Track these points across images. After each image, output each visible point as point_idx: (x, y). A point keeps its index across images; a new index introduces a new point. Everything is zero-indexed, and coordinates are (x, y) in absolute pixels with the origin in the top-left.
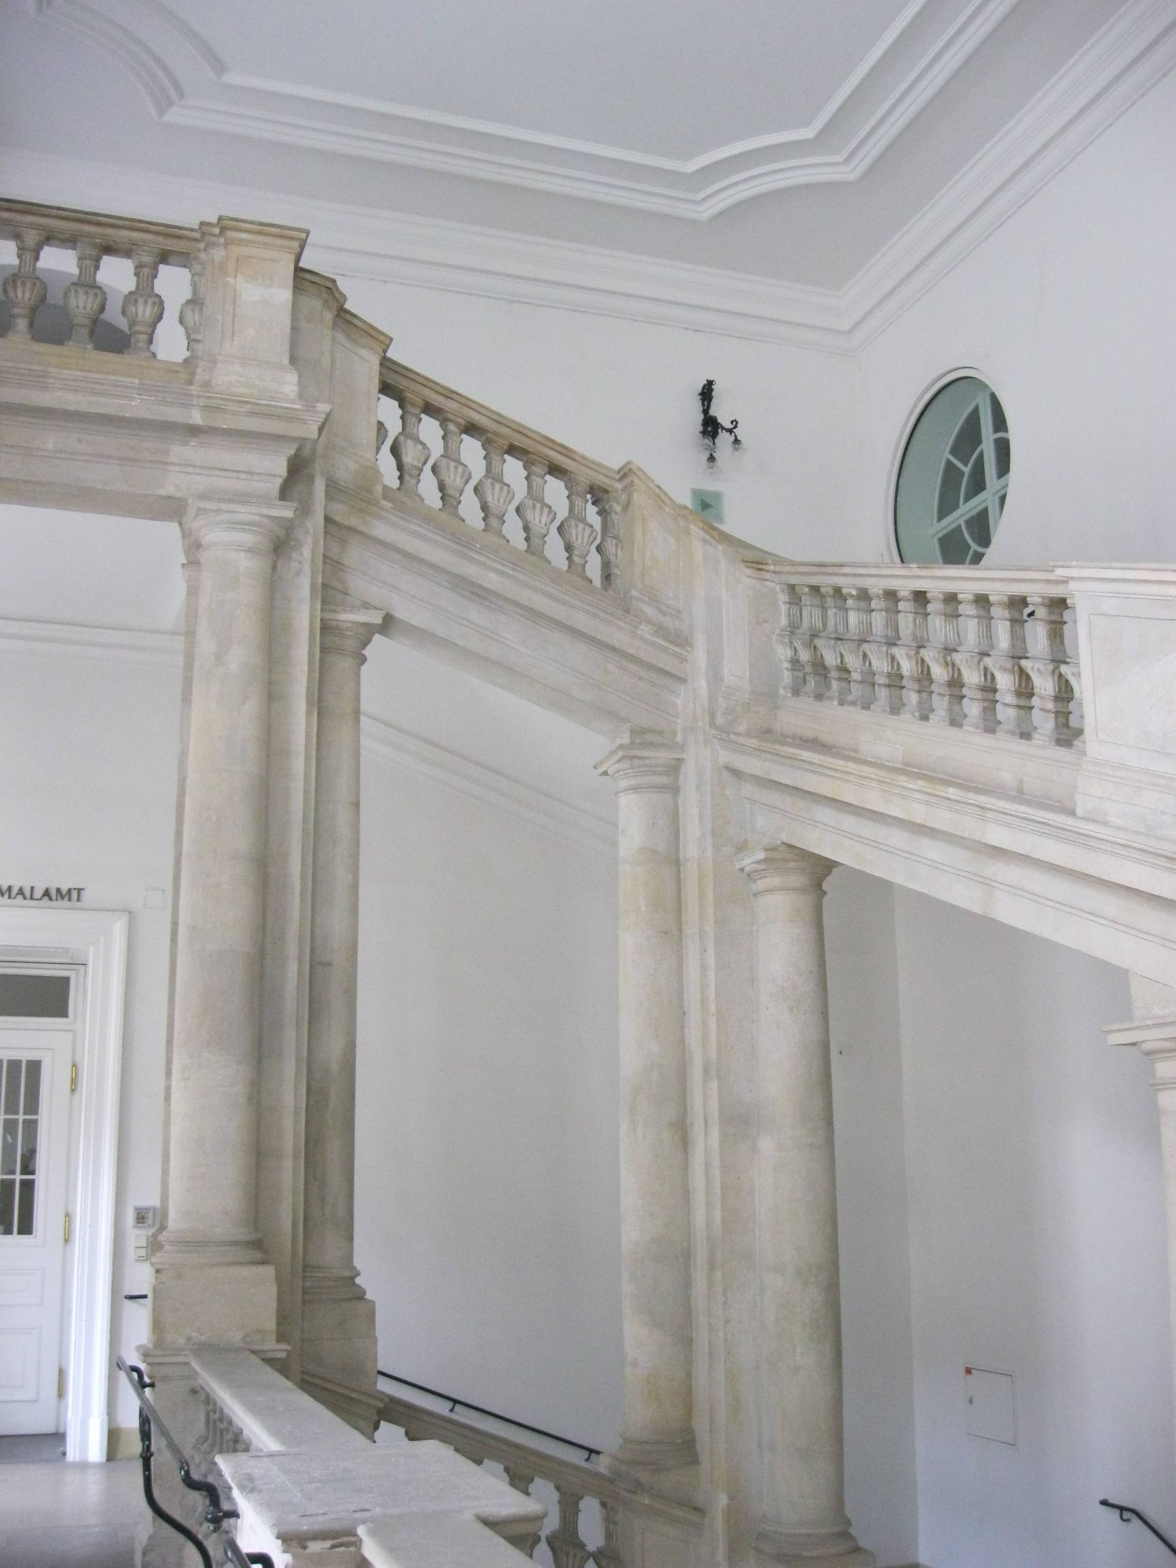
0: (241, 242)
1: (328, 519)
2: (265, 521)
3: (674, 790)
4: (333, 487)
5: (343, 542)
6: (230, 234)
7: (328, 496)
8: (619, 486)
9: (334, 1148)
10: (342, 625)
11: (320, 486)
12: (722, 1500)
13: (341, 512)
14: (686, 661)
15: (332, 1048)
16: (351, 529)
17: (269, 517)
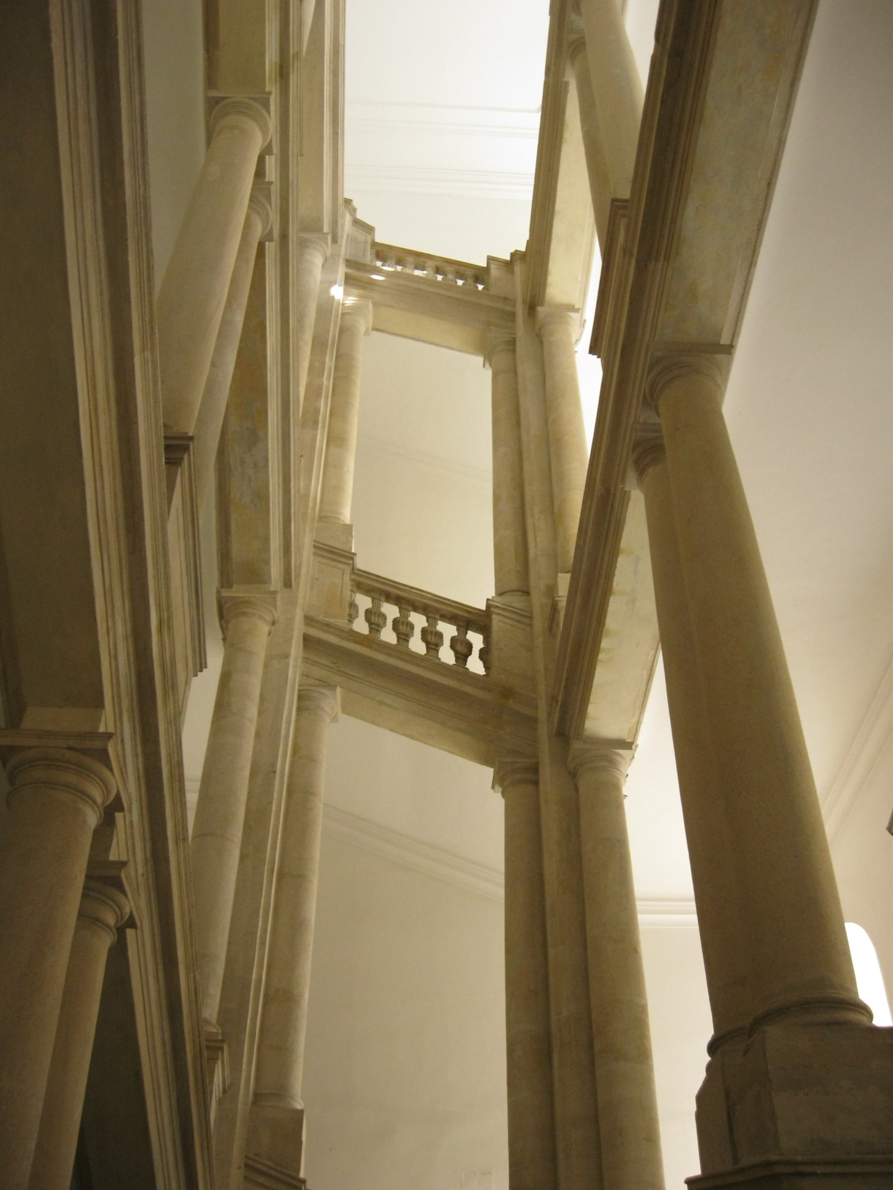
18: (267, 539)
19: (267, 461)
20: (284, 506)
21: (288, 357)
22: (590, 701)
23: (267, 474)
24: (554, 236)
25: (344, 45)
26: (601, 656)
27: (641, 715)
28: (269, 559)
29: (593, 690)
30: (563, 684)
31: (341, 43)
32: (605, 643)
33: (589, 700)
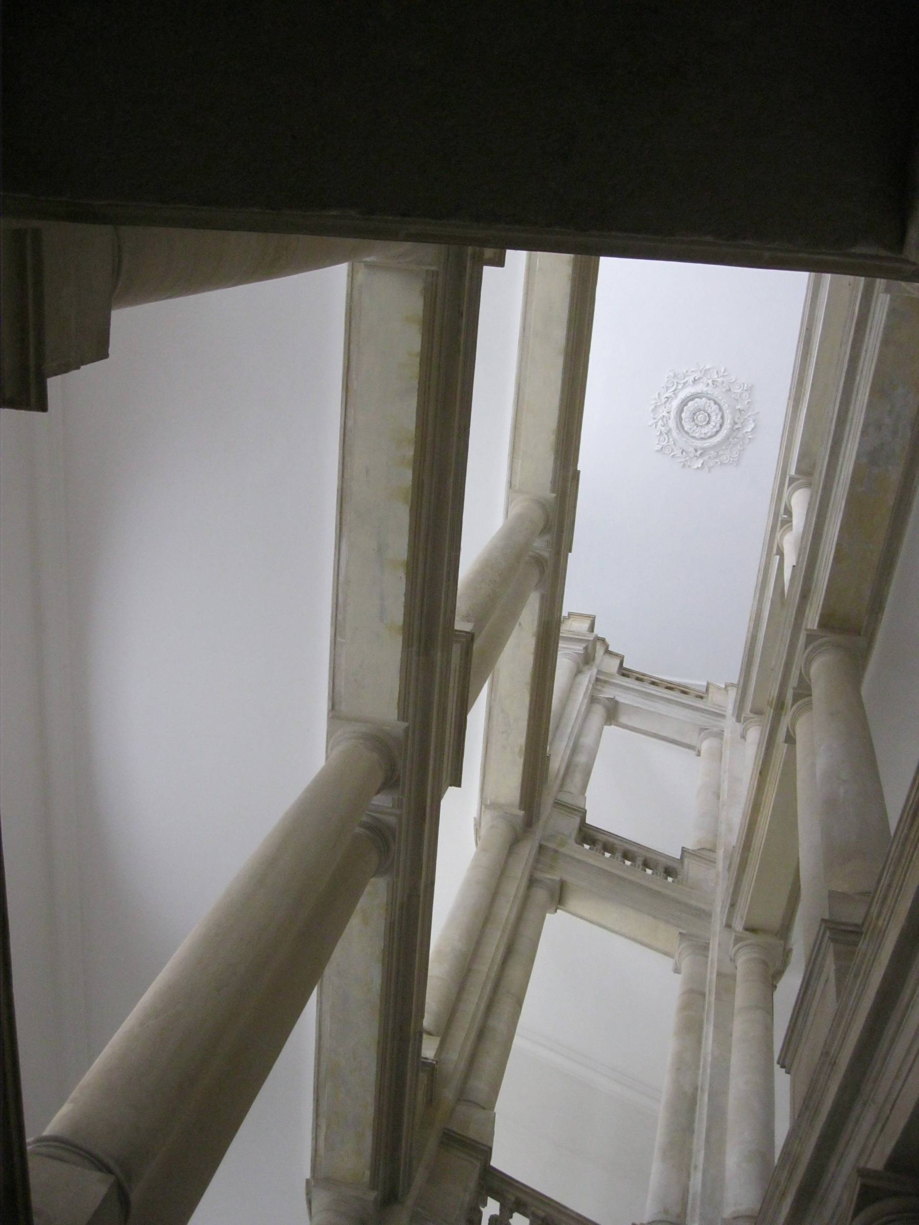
0: (574, 618)
1: (597, 680)
2: (574, 654)
3: (722, 739)
4: (599, 672)
5: (603, 687)
6: (571, 616)
7: (597, 674)
8: (706, 695)
9: (578, 778)
10: (600, 698)
11: (594, 671)
12: (723, 850)
13: (601, 677)
14: (725, 711)
15: (582, 759)
16: (605, 682)
17: (576, 653)
18: (886, 341)
19: (864, 432)
20: (862, 341)
21: (822, 497)
22: (418, 360)
23: (867, 418)
24: (565, 325)
25: (789, 399)
26: (409, 452)
27: (350, 292)
28: (888, 316)
29: (415, 383)
30: (464, 319)
31: (791, 409)
32: (407, 476)
33: (419, 383)
